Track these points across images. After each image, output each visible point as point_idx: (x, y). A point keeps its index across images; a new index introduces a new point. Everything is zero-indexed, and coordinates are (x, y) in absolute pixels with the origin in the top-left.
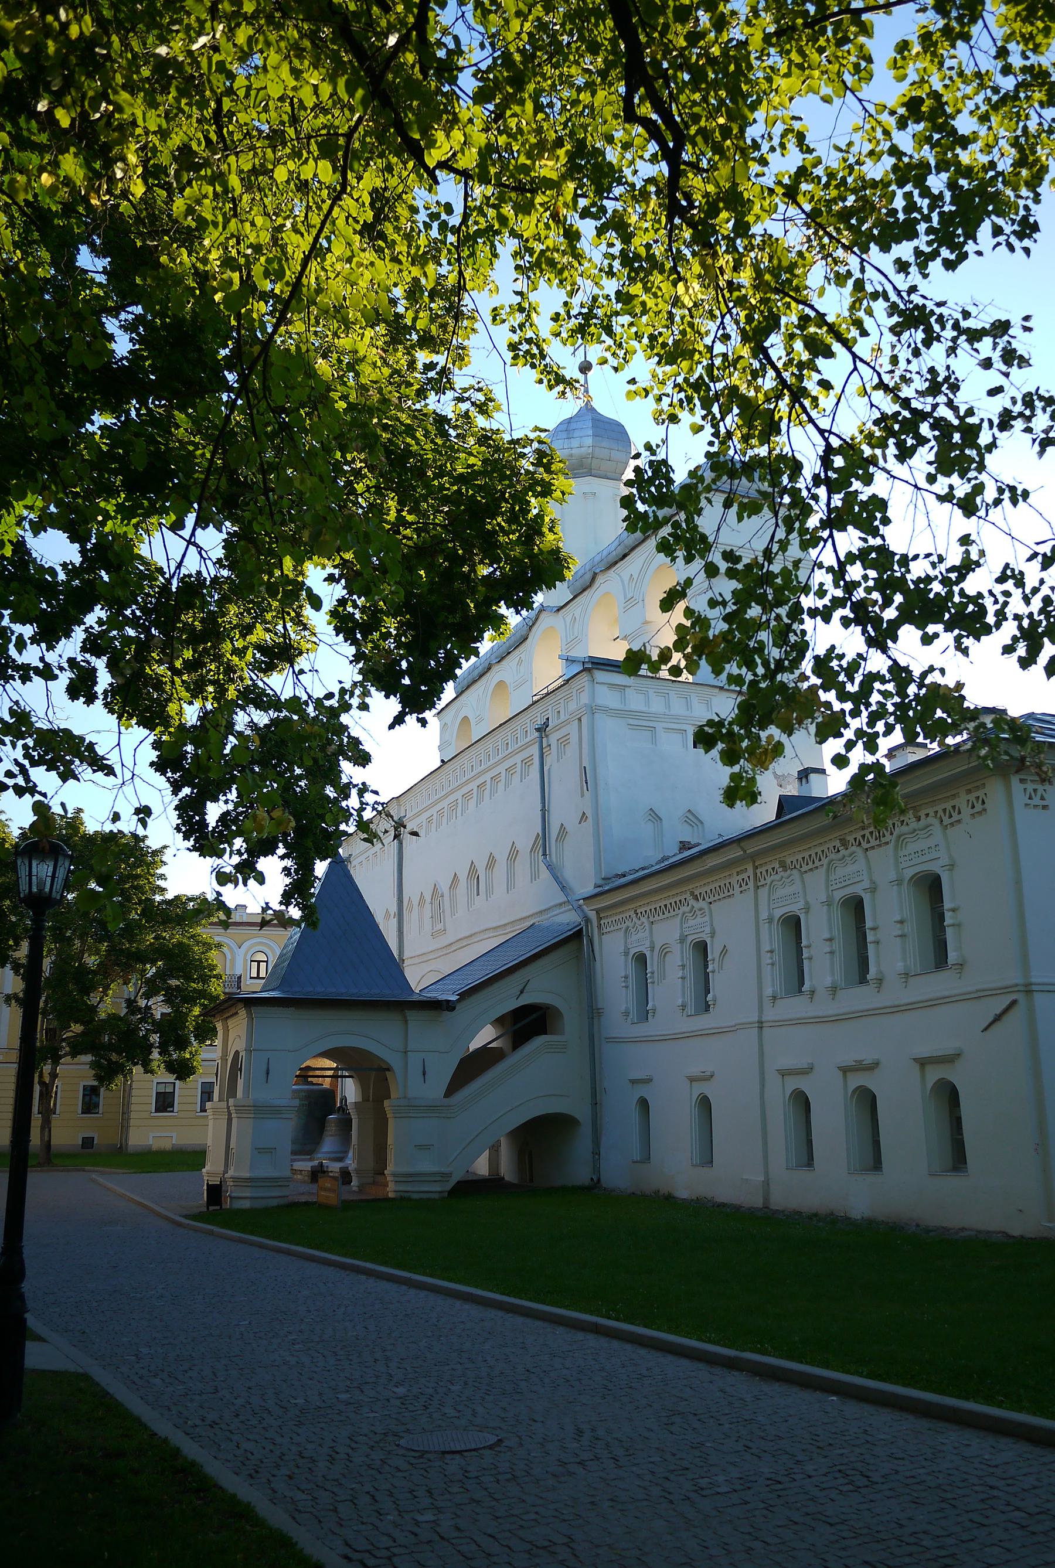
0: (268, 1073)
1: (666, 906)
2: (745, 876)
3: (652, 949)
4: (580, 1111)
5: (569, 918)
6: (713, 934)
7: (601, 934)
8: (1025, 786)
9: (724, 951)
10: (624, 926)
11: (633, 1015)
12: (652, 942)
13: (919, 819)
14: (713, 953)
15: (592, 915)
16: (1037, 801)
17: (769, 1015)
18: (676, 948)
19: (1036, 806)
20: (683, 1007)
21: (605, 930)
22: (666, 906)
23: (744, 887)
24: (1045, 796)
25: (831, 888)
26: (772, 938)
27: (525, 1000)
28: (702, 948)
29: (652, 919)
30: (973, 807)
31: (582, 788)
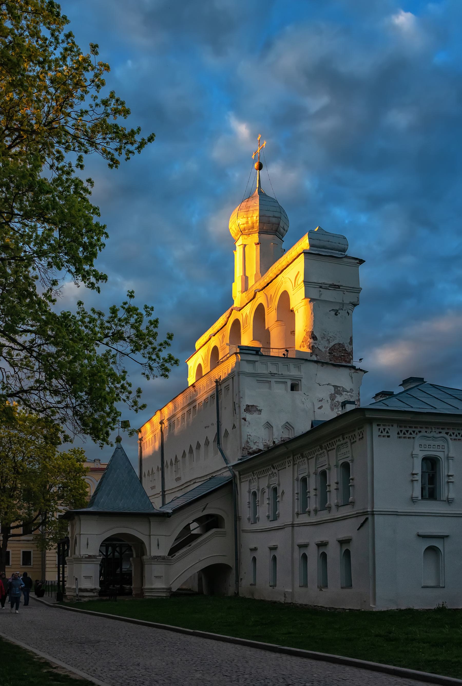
0: (88, 544)
1: (264, 470)
2: (290, 459)
3: (258, 490)
4: (232, 563)
5: (228, 474)
6: (279, 485)
7: (241, 482)
8: (379, 427)
9: (283, 493)
10: (249, 479)
11: (252, 520)
12: (258, 487)
13: (344, 439)
14: (279, 493)
15: (237, 473)
16: (385, 434)
17: (297, 521)
18: (267, 490)
19: (384, 436)
20: (268, 517)
21: (242, 481)
22: (264, 470)
23: (290, 464)
25: (317, 467)
26: (298, 488)
27: (206, 512)
28: (275, 490)
29: (259, 476)
30: (360, 436)
31: (233, 413)
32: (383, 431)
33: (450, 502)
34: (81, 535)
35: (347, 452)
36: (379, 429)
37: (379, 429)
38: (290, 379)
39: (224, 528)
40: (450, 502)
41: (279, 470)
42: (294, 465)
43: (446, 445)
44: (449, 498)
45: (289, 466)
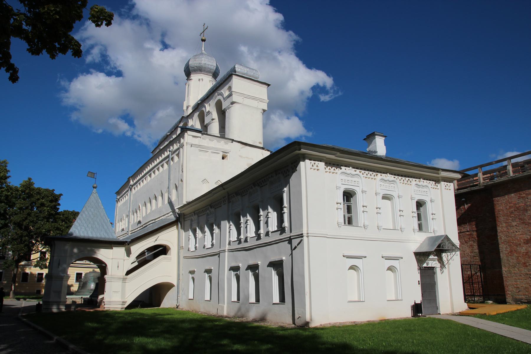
19: (314, 169)
24: (318, 165)
32: (314, 164)
33: (366, 228)
34: (112, 274)
35: (279, 185)
36: (311, 163)
37: (311, 163)
38: (222, 152)
39: (170, 255)
40: (366, 228)
41: (215, 209)
42: (229, 202)
43: (360, 180)
44: (365, 225)
45: (224, 204)
